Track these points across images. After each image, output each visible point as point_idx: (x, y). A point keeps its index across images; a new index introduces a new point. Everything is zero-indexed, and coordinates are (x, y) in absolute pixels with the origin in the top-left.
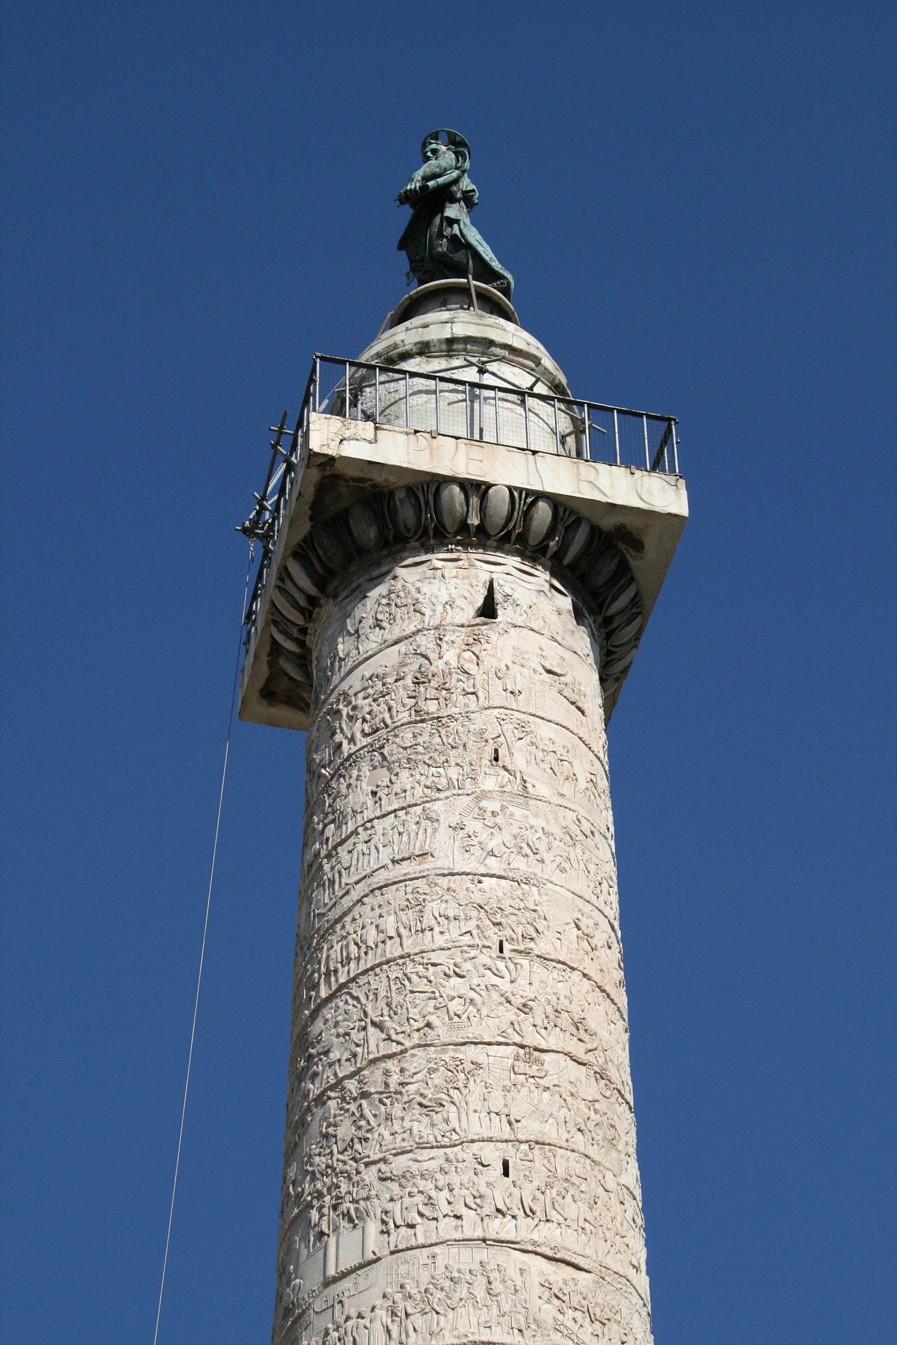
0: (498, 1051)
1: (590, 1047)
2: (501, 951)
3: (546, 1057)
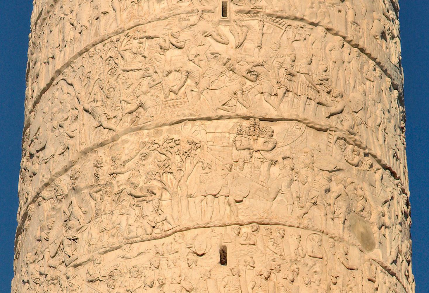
0: (217, 127)
1: (333, 110)
2: (224, 13)
3: (277, 127)
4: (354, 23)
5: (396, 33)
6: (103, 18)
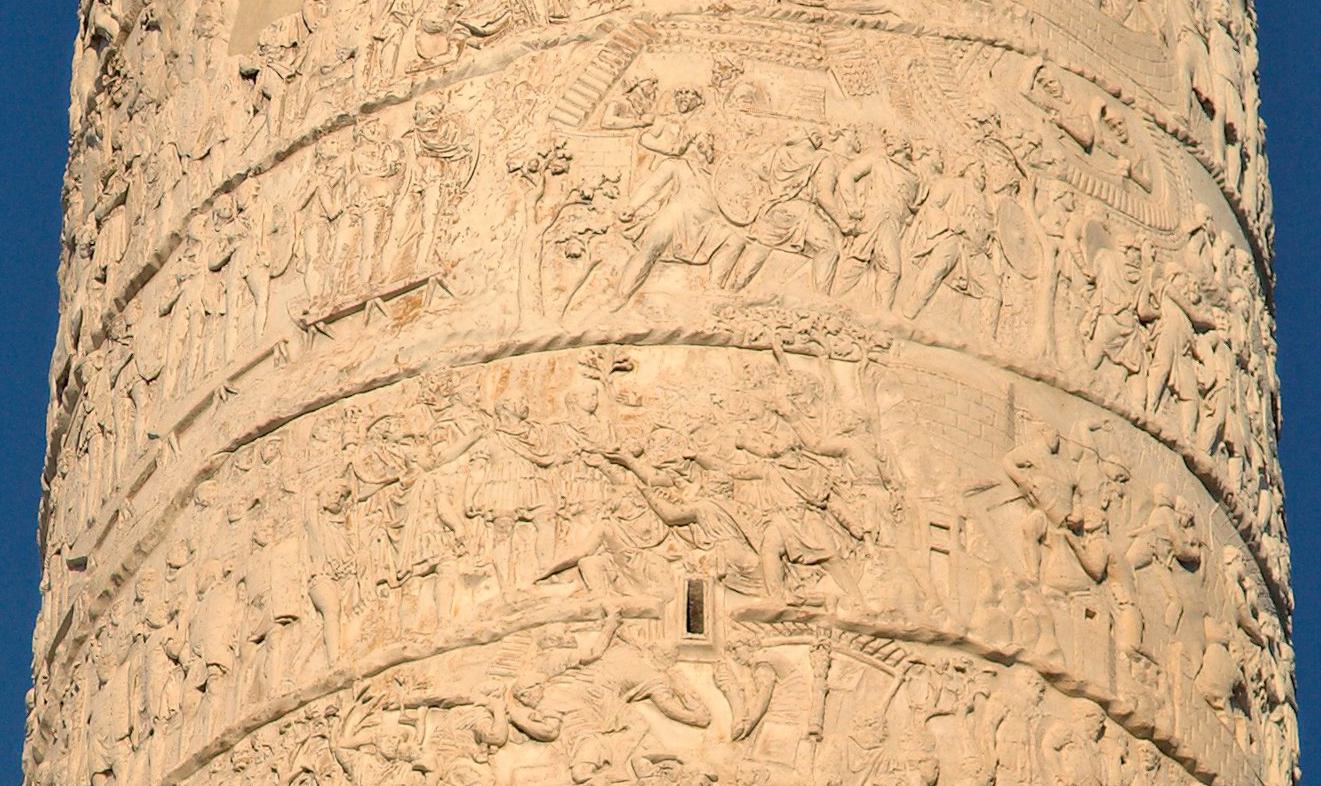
2: (694, 620)
4: (1139, 654)
5: (1281, 687)
6: (280, 638)
